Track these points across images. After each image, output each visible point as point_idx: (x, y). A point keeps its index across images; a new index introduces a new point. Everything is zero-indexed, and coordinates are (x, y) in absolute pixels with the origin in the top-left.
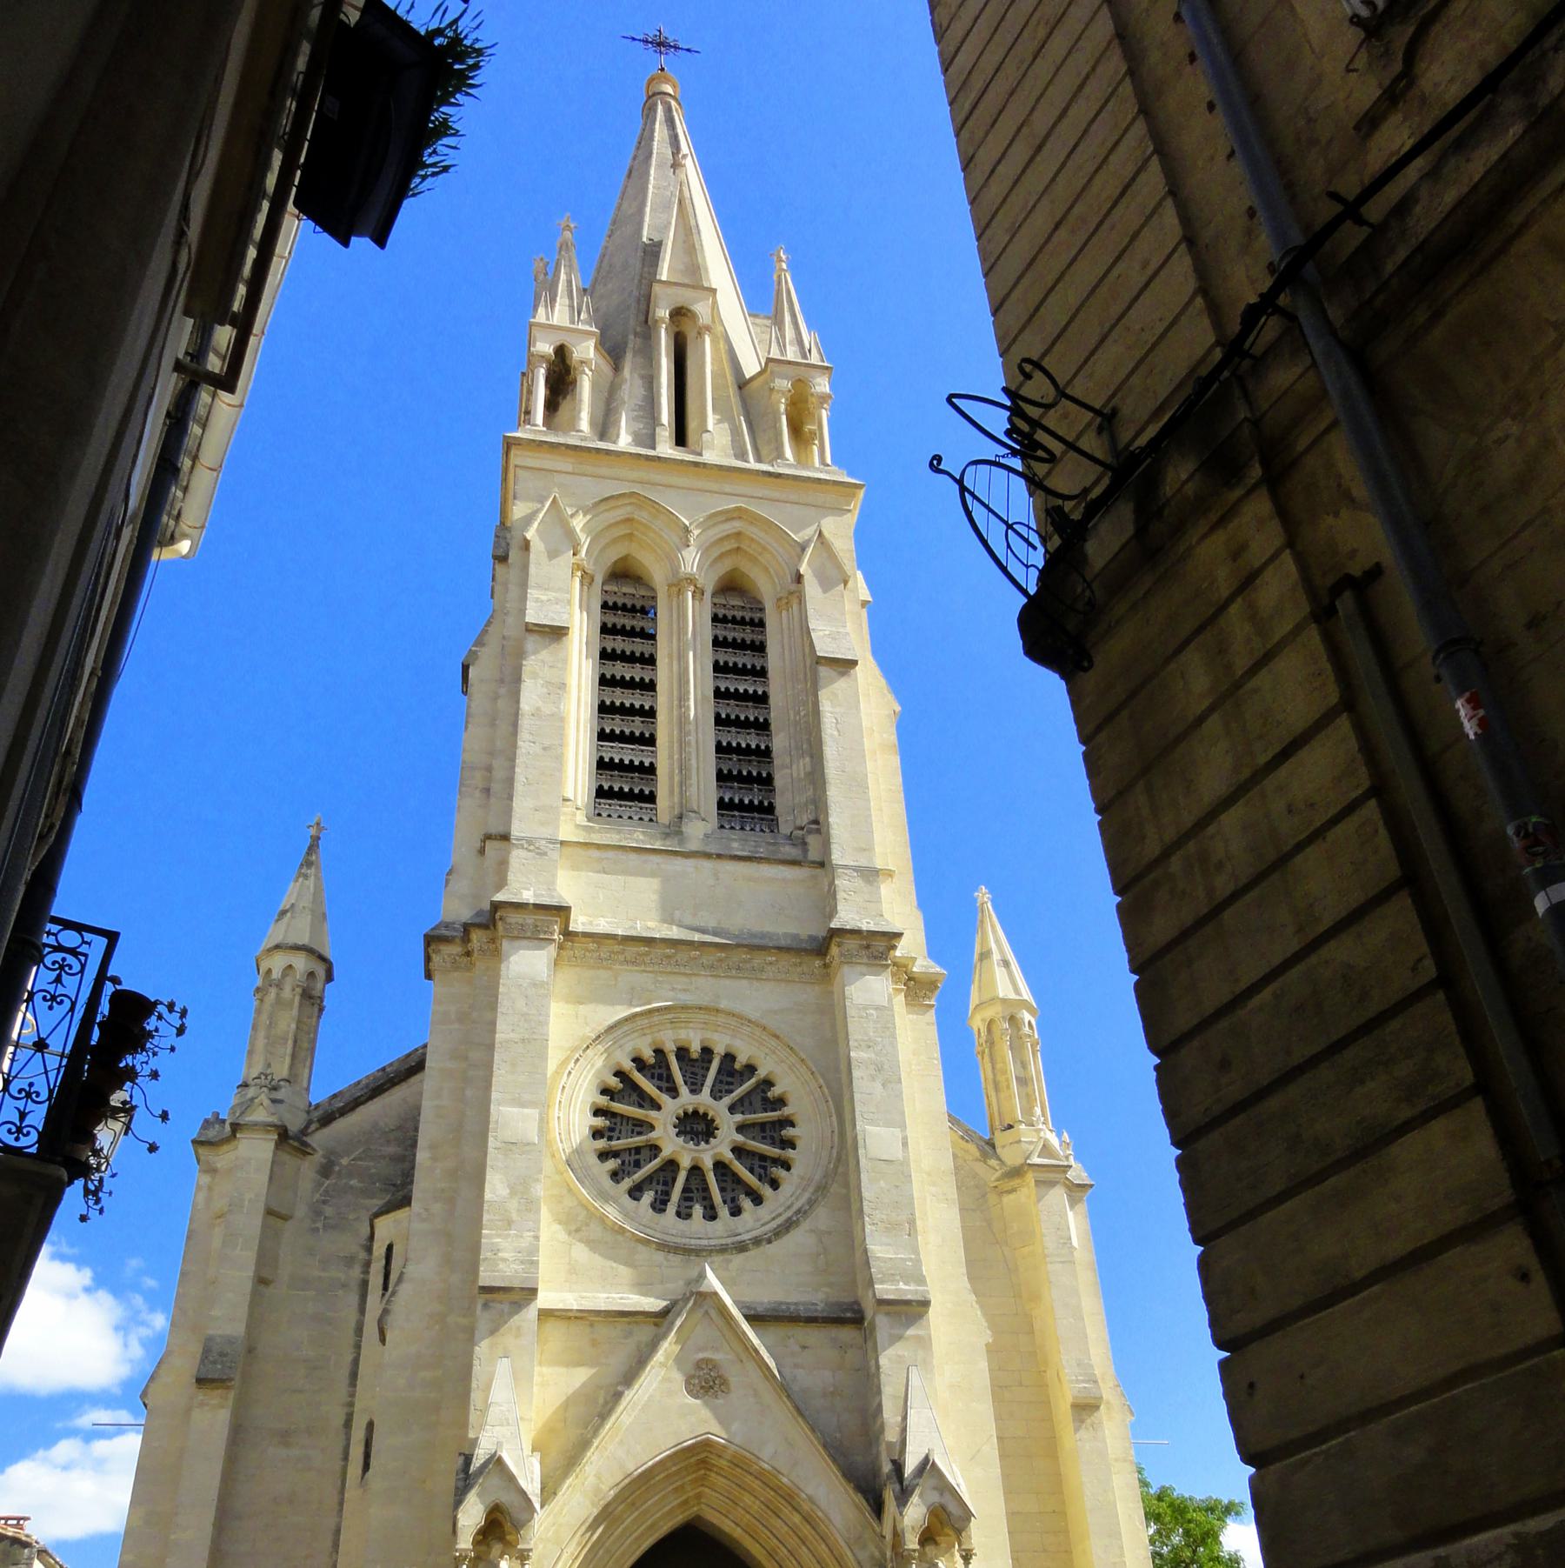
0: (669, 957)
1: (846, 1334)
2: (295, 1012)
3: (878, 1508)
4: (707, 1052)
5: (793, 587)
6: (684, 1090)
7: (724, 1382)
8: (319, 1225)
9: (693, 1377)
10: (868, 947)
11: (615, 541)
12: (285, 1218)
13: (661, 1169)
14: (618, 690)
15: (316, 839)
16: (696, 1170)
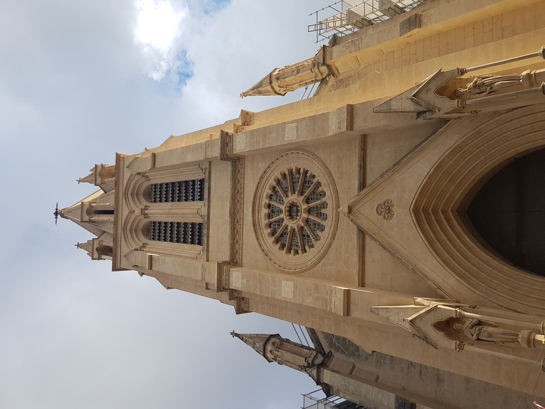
0: (238, 222)
1: (369, 142)
2: (284, 352)
3: (444, 121)
4: (269, 206)
5: (142, 175)
6: (281, 216)
7: (387, 201)
8: (357, 354)
9: (384, 217)
10: (227, 144)
12: (354, 367)
14: (173, 235)
16: (309, 211)
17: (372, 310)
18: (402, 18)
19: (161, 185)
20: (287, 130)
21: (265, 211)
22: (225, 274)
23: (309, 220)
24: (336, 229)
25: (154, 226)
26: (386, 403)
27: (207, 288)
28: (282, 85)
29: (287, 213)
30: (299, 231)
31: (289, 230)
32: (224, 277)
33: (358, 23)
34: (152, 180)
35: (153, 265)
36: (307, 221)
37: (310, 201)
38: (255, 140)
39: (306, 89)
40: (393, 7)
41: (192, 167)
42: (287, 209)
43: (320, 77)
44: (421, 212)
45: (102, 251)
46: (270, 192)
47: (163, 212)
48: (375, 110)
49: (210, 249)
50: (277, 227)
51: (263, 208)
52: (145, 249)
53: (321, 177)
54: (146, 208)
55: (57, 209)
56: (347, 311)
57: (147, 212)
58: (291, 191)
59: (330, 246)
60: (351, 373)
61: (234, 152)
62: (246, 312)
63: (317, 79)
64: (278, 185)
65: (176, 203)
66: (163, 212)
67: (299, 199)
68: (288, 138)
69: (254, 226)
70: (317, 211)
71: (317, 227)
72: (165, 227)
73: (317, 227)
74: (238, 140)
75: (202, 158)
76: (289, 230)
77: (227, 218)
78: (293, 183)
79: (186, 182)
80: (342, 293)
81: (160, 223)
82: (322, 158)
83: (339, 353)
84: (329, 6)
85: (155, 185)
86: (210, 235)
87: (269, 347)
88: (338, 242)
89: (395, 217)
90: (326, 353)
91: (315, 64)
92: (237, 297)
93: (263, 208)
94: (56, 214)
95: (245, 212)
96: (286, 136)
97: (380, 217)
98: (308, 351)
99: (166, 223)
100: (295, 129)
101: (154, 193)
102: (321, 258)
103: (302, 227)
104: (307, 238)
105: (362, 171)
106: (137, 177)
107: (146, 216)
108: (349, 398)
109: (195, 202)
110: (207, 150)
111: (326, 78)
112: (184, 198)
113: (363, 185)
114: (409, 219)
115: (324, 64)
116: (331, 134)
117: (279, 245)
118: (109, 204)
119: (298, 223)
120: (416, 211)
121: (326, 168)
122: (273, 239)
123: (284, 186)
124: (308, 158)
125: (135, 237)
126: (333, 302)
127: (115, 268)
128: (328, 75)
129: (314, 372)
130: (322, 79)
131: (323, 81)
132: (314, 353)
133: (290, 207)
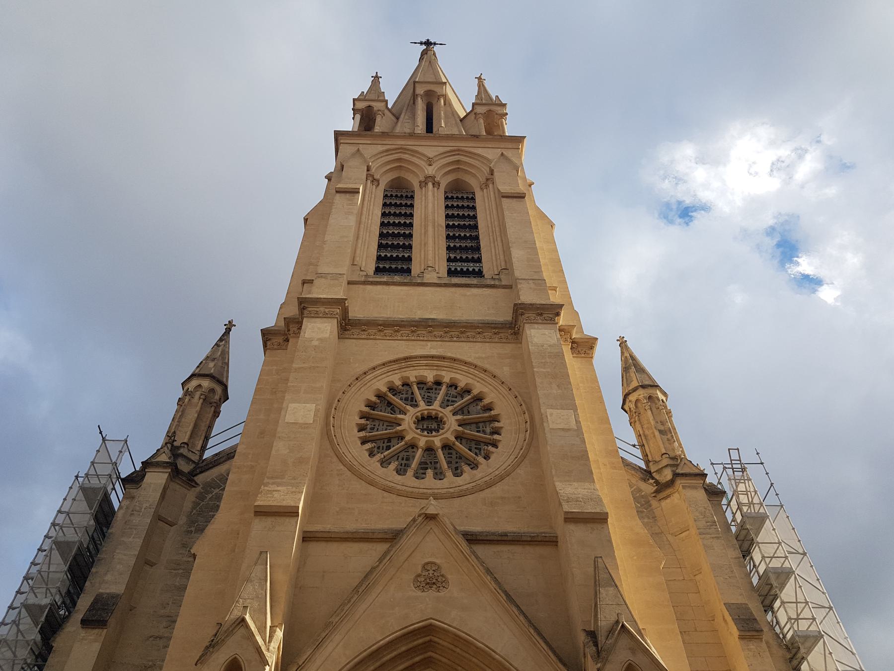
0: (413, 332)
2: (198, 408)
4: (438, 383)
7: (446, 581)
8: (193, 529)
9: (419, 576)
10: (541, 314)
11: (391, 170)
13: (405, 449)
14: (391, 227)
15: (228, 331)
16: (429, 450)
17: (263, 555)
18: (755, 607)
19: (474, 208)
20: (565, 412)
21: (430, 376)
22: (327, 310)
23: (415, 450)
24: (399, 494)
25: (407, 196)
26: (108, 577)
27: (304, 282)
28: (639, 405)
29: (426, 412)
30: (396, 432)
31: (400, 416)
32: (322, 309)
33: (744, 532)
34: (481, 193)
35: (343, 195)
36: (413, 446)
37: (447, 451)
38: (548, 360)
39: (634, 446)
40: (773, 592)
41: (502, 257)
42: (434, 413)
43: (653, 468)
44: (428, 638)
45: (367, 113)
46: (462, 385)
47: (429, 214)
48: (600, 560)
49: (369, 287)
50: (404, 396)
51: (435, 373)
52: (369, 182)
53: (487, 469)
54: (436, 184)
55: (435, 44)
56: (262, 513)
57: (430, 185)
58: (464, 420)
59: (371, 483)
60: (160, 519)
61: (527, 326)
62: (265, 345)
63: (651, 464)
64: (472, 398)
65: (443, 232)
66: (429, 214)
67: (449, 432)
68: (551, 415)
69: (406, 359)
70: (429, 463)
71: (404, 462)
72: (406, 215)
73: (404, 462)
74: (547, 332)
75: (517, 274)
76: (400, 416)
77: (419, 315)
78: (477, 423)
79: (478, 249)
80: (293, 504)
81: (412, 206)
82: (518, 471)
83: (194, 499)
84: (772, 484)
85: (473, 199)
86: (392, 287)
87: (206, 383)
88: (380, 498)
89: (419, 593)
90: (195, 478)
91: (676, 460)
92: (289, 330)
93: (435, 373)
94: (428, 43)
95: (429, 344)
96: (555, 412)
97: (420, 568)
98: (199, 448)
99: (411, 215)
100: (566, 427)
101: (460, 196)
102: (350, 468)
103: (402, 438)
104: (385, 445)
105: (496, 538)
106: (486, 170)
107: (423, 184)
108: (119, 515)
109: (445, 263)
110: (531, 282)
111: (653, 478)
112: (452, 245)
113: (472, 539)
114: (415, 618)
115: (676, 475)
116: (559, 485)
117: (374, 399)
118: (442, 125)
119: (410, 432)
120: (428, 629)
121: (502, 478)
122: (384, 389)
123: (471, 408)
124: (518, 447)
125: (388, 167)
126: (279, 488)
127: (338, 135)
128: (657, 482)
129: (164, 458)
130: (650, 473)
131: (647, 474)
132: (195, 458)
133: (436, 418)
